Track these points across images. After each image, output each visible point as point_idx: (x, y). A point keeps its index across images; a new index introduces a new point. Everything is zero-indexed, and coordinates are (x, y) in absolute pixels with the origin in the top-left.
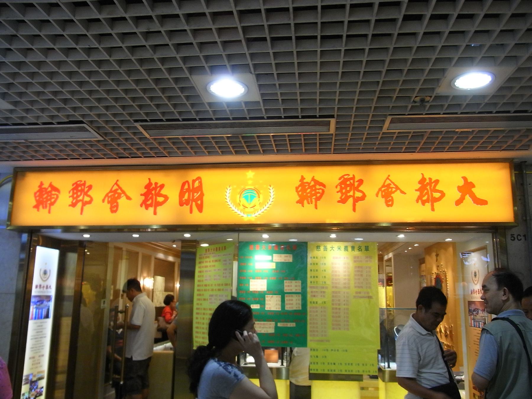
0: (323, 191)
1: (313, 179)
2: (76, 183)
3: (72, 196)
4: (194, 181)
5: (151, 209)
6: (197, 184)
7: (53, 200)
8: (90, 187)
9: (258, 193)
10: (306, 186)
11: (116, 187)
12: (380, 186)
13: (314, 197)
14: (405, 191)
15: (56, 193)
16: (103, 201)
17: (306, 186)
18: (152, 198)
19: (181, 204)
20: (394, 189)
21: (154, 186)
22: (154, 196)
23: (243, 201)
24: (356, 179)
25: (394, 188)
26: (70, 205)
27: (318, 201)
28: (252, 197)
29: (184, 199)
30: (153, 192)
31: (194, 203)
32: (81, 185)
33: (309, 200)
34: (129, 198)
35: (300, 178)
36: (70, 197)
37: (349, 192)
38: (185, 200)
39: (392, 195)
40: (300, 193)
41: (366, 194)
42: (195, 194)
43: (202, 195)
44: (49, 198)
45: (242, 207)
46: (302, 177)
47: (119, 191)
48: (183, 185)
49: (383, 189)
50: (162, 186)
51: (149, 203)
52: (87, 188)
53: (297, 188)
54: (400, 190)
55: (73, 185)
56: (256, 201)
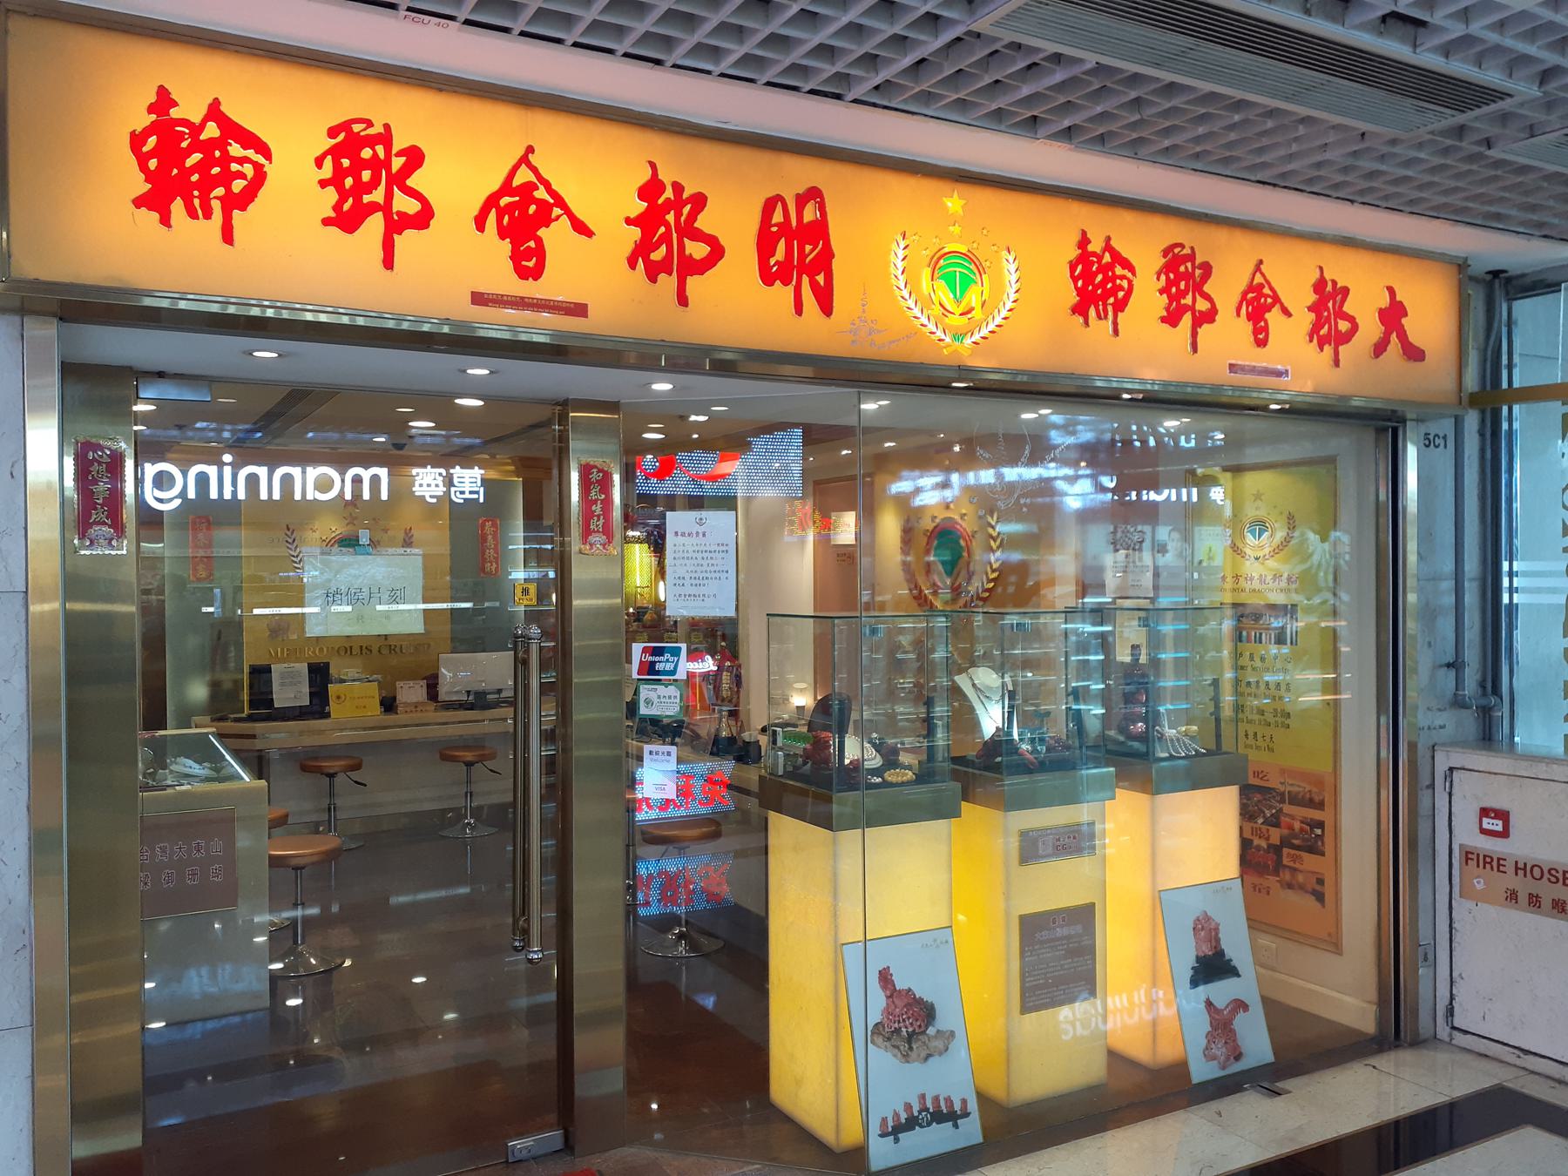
0: (1130, 283)
1: (1108, 247)
2: (346, 126)
3: (335, 181)
4: (801, 201)
5: (668, 282)
6: (810, 214)
7: (238, 186)
8: (415, 158)
9: (981, 271)
10: (1093, 263)
11: (525, 175)
12: (1243, 286)
13: (1111, 300)
14: (1291, 309)
15: (260, 159)
16: (480, 223)
17: (1093, 263)
18: (666, 238)
19: (767, 278)
20: (1269, 300)
21: (669, 193)
22: (675, 235)
23: (944, 295)
24: (1198, 261)
25: (1269, 296)
26: (327, 222)
27: (1119, 314)
28: (967, 283)
29: (772, 261)
30: (670, 217)
31: (805, 280)
32: (371, 141)
33: (1101, 307)
34: (581, 228)
35: (1076, 237)
36: (323, 184)
37: (1183, 294)
38: (777, 263)
39: (1267, 316)
40: (1080, 283)
41: (1218, 306)
42: (808, 248)
43: (827, 256)
44: (216, 170)
45: (937, 310)
46: (1084, 233)
47: (541, 193)
48: (769, 206)
49: (1250, 295)
50: (699, 202)
51: (658, 255)
52: (402, 160)
53: (1073, 267)
54: (1282, 304)
55: (332, 132)
56: (974, 298)
